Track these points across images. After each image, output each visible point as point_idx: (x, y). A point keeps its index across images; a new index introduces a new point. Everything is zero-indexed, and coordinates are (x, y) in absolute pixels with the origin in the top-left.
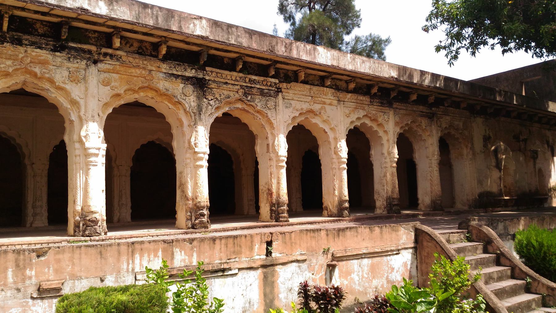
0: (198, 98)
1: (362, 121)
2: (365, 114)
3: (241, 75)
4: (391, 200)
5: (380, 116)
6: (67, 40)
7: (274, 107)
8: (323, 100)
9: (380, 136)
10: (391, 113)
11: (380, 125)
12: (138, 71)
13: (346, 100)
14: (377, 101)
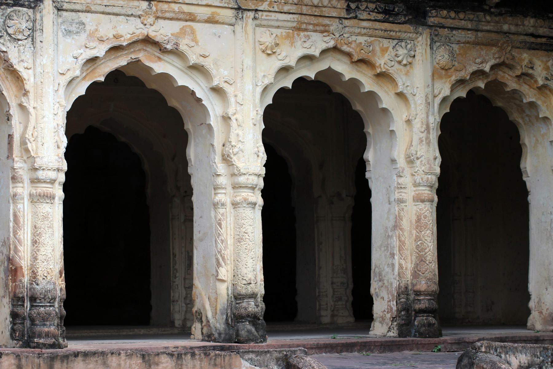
1: (323, 66)
2: (331, 44)
4: (412, 297)
5: (384, 50)
7: (27, 33)
8: (186, 8)
9: (385, 110)
10: (422, 41)
11: (383, 76)
14: (372, 6)
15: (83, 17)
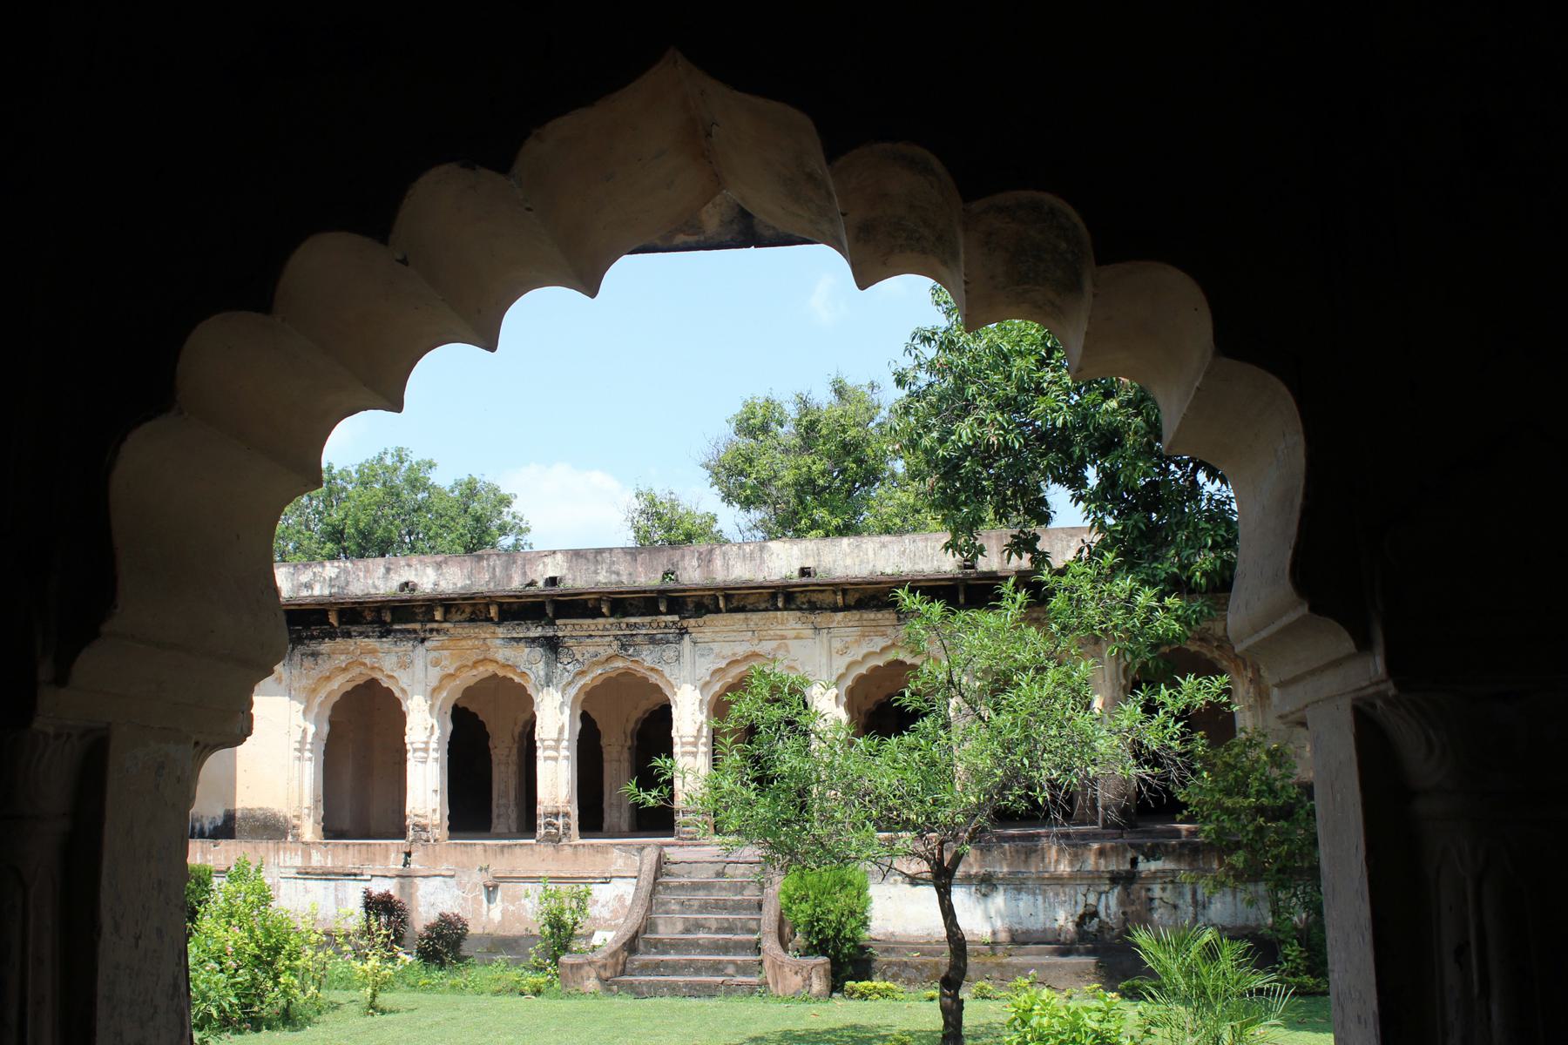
0: (547, 664)
1: (891, 656)
3: (612, 620)
6: (393, 622)
12: (470, 643)
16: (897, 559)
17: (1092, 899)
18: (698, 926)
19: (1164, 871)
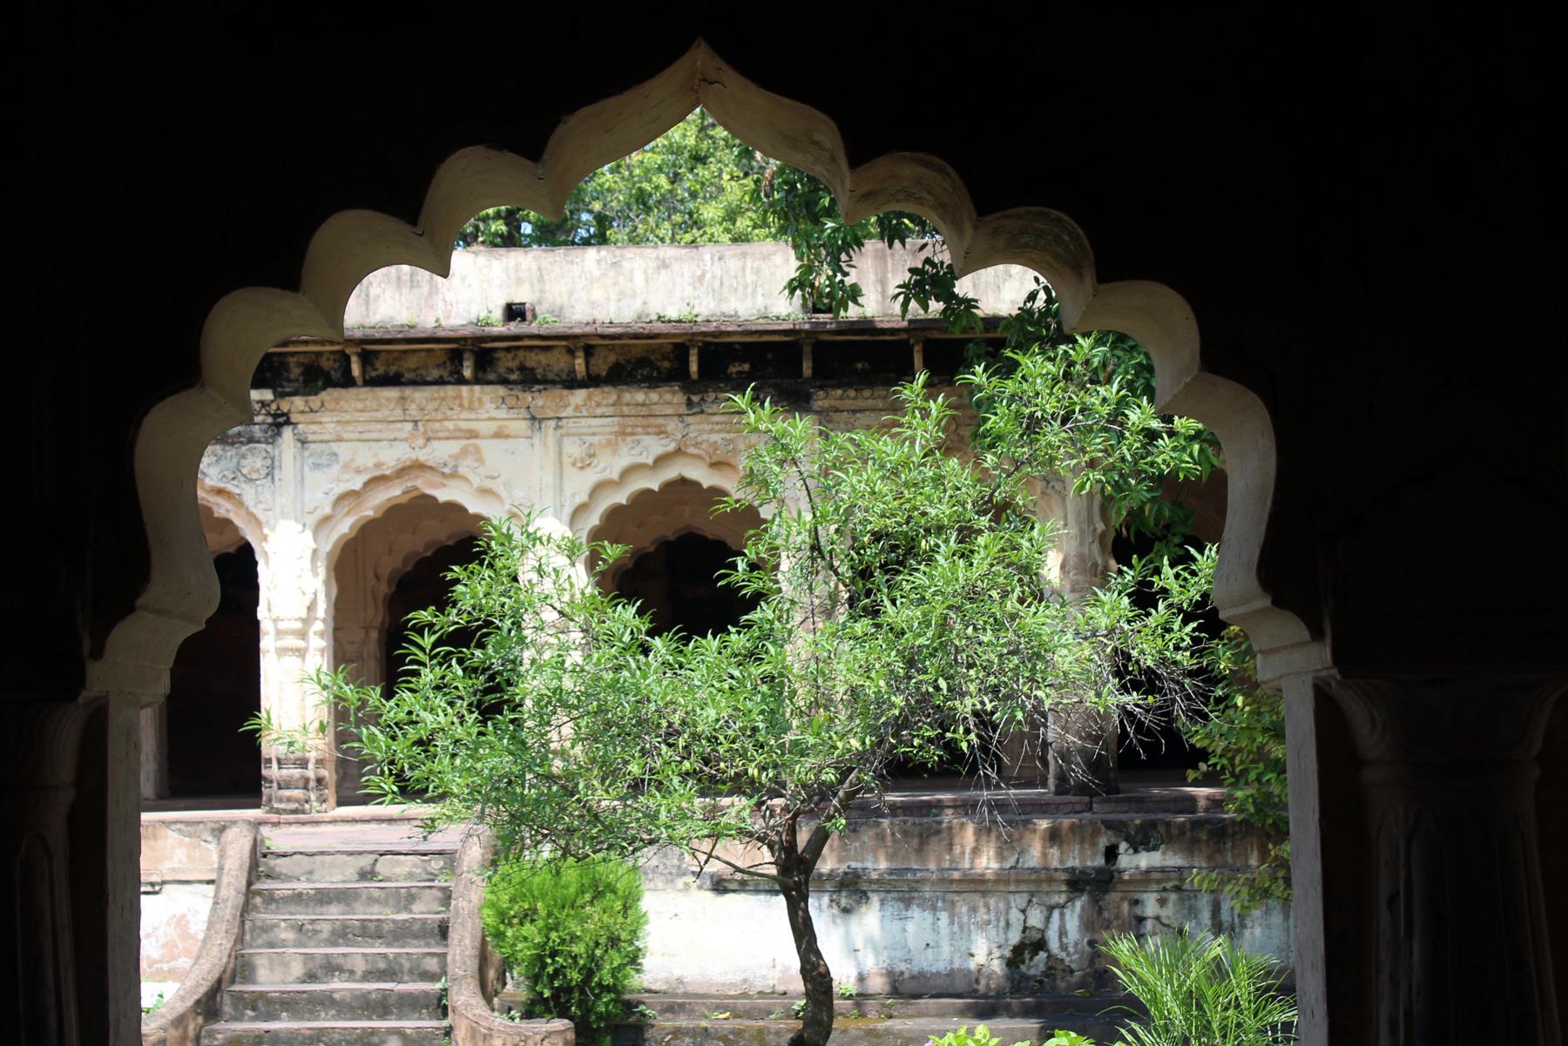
1: (671, 473)
2: (672, 447)
8: (463, 425)
13: (569, 412)
15: (335, 447)
16: (688, 291)
17: (1036, 918)
18: (332, 968)
19: (1163, 870)
